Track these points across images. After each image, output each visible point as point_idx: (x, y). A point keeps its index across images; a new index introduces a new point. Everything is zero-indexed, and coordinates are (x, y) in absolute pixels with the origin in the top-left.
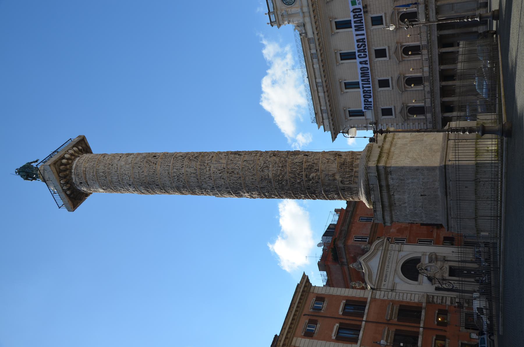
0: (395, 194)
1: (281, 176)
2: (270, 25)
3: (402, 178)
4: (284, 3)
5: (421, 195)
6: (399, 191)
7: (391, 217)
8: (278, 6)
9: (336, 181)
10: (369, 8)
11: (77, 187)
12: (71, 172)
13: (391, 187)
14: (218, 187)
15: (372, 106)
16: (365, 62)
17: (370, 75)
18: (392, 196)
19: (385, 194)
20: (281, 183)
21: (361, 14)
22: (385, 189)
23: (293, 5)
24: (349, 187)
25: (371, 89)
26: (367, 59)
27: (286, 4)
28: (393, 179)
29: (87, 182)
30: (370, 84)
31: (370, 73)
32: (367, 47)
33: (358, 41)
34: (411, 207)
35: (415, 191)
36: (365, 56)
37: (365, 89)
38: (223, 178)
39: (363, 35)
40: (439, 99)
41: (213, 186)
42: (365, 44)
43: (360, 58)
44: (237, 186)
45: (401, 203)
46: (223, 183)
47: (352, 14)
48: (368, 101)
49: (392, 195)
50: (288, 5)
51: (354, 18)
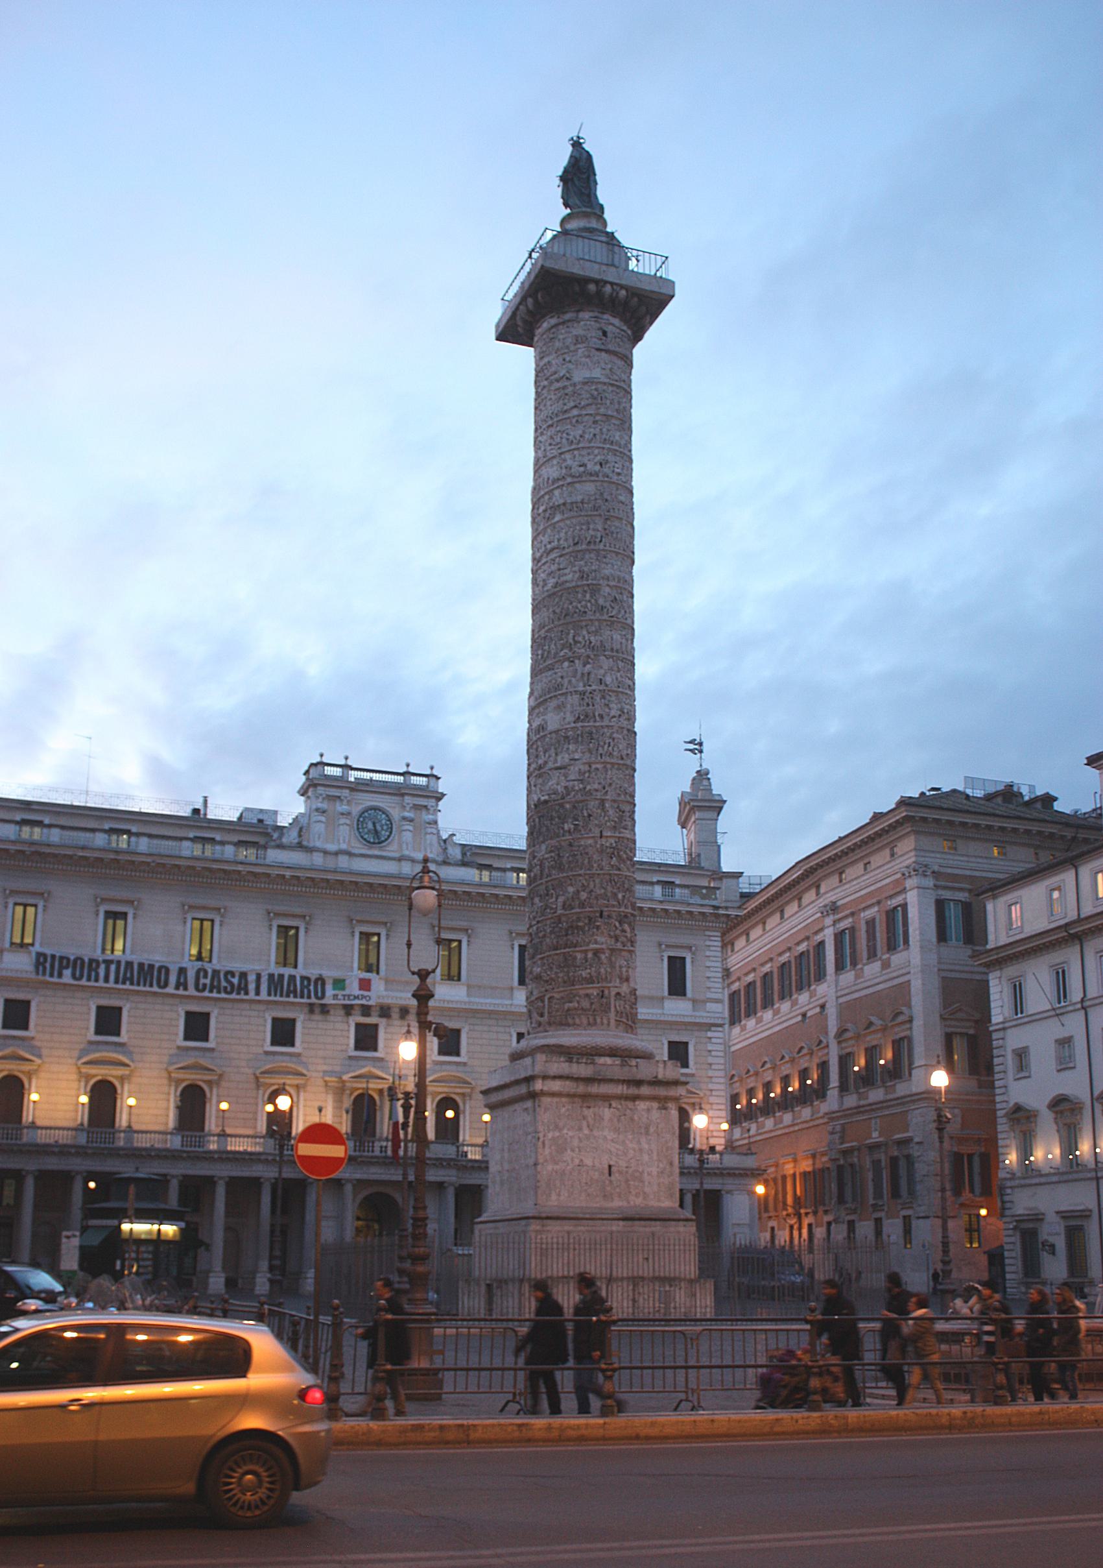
0: (612, 1110)
1: (625, 856)
2: (318, 759)
3: (652, 1130)
4: (363, 813)
5: (610, 1166)
6: (619, 1120)
7: (553, 1094)
8: (361, 794)
9: (618, 981)
10: (317, 1017)
11: (591, 314)
12: (625, 321)
13: (630, 1104)
14: (603, 697)
15: (48, 978)
16: (181, 984)
17: (141, 988)
18: (607, 1104)
19: (620, 1089)
20: (613, 853)
21: (309, 997)
22: (633, 1091)
23: (356, 832)
24: (610, 1008)
25: (101, 983)
26: (191, 991)
27: (360, 816)
28: (648, 1110)
29: (607, 351)
30: (117, 982)
31: (148, 989)
32: (223, 995)
33: (243, 975)
34: (580, 1140)
35: (619, 1153)
36: (201, 987)
37: (103, 967)
38: (620, 716)
39: (258, 993)
40: (83, 1168)
41: (606, 685)
42: (231, 993)
43: (198, 972)
44: (606, 746)
45: (590, 1119)
46: (613, 713)
47: (313, 973)
48: (61, 968)
49: (610, 1105)
50: (358, 820)
51: (303, 978)
